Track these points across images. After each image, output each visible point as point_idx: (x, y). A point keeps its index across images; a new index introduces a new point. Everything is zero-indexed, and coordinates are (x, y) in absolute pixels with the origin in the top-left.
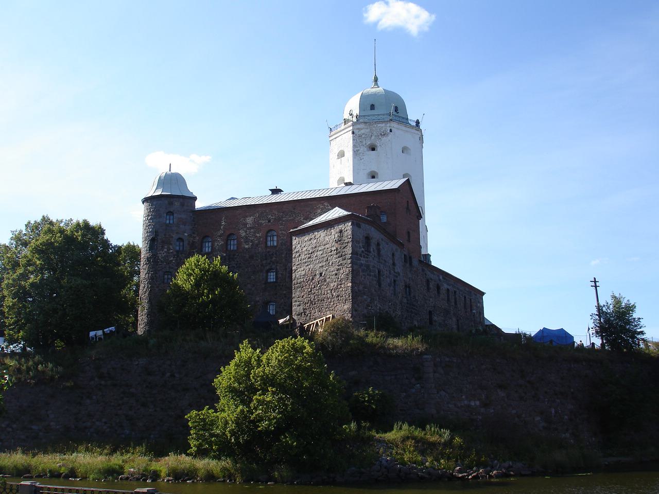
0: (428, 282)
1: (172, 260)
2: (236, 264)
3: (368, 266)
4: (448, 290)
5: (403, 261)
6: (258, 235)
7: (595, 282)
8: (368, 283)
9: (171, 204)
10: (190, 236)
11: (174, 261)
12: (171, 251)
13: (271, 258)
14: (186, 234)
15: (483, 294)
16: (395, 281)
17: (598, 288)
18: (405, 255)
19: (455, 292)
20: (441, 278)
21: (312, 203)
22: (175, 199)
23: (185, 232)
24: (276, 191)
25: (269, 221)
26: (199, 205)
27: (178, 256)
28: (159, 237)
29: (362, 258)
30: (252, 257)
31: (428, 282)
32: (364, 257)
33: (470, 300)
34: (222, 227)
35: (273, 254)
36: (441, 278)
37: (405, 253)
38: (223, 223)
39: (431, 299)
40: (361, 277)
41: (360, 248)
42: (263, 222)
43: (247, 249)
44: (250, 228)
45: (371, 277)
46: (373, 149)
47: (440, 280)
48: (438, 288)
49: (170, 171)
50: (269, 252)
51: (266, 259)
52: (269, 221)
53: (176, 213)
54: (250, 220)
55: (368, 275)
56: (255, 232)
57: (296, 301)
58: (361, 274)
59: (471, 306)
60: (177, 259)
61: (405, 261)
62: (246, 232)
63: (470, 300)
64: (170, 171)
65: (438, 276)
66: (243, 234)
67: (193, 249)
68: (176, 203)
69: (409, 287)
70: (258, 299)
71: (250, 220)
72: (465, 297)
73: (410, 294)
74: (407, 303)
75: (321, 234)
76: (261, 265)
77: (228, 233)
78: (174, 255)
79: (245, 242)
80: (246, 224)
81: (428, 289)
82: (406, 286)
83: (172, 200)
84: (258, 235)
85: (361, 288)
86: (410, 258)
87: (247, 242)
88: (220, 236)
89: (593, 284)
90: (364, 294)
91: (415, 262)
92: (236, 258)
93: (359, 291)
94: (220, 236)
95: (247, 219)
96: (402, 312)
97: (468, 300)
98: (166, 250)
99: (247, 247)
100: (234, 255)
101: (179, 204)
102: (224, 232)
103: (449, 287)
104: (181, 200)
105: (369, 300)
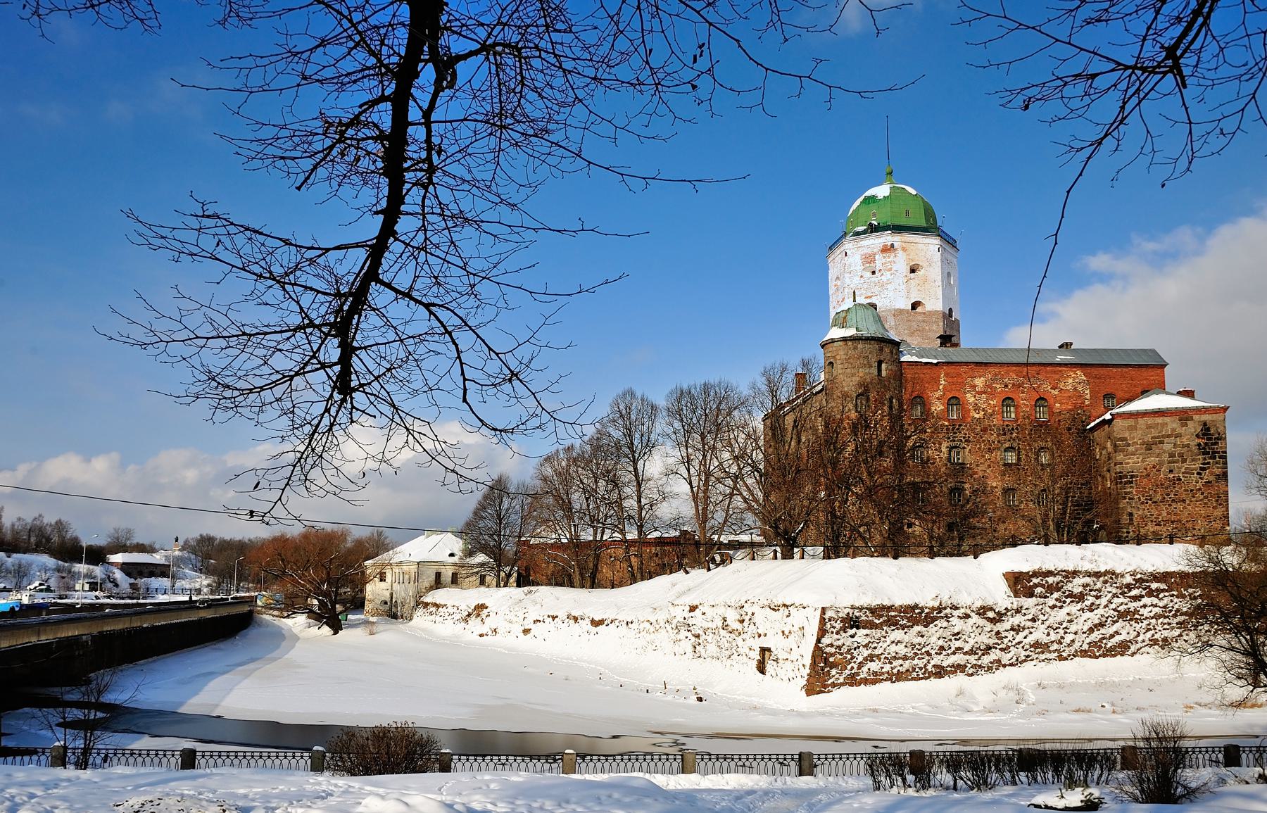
2: (964, 438)
6: (992, 402)
9: (881, 350)
13: (1012, 434)
21: (1060, 369)
25: (1006, 386)
34: (941, 387)
35: (1013, 429)
38: (943, 382)
42: (998, 386)
44: (982, 393)
50: (1007, 426)
51: (1005, 434)
52: (1006, 386)
54: (979, 382)
56: (987, 399)
57: (1125, 498)
62: (975, 396)
66: (972, 400)
76: (999, 442)
79: (975, 410)
80: (974, 387)
84: (992, 402)
87: (977, 409)
88: (938, 399)
92: (963, 429)
94: (938, 399)
99: (977, 416)
100: (960, 425)
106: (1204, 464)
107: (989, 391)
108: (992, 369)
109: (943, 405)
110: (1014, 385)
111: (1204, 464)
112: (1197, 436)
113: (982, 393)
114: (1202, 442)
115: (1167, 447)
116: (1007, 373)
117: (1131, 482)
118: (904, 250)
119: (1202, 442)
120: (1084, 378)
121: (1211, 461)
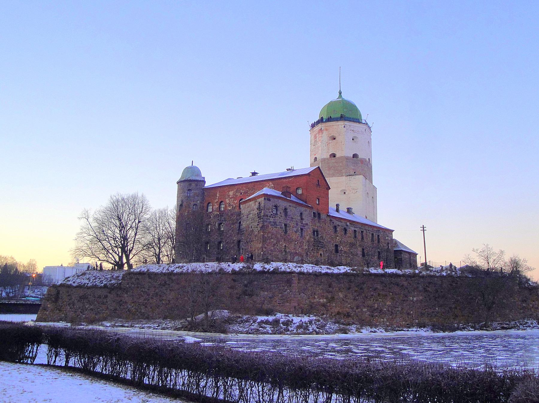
0: (335, 227)
2: (224, 219)
3: (275, 223)
4: (355, 231)
5: (312, 216)
6: (235, 202)
7: (423, 227)
8: (275, 232)
9: (190, 185)
10: (201, 203)
15: (393, 231)
16: (302, 229)
17: (425, 231)
18: (314, 213)
19: (362, 232)
20: (348, 224)
21: (263, 183)
24: (254, 174)
25: (241, 194)
26: (207, 185)
28: (184, 204)
29: (271, 218)
30: (232, 215)
31: (335, 227)
32: (273, 217)
33: (378, 236)
36: (348, 224)
37: (315, 212)
39: (337, 237)
40: (270, 229)
41: (270, 212)
42: (238, 194)
43: (230, 210)
44: (232, 198)
45: (278, 229)
46: (334, 139)
47: (347, 225)
48: (345, 230)
49: (192, 165)
52: (241, 194)
53: (193, 190)
54: (231, 193)
55: (275, 227)
56: (234, 200)
58: (270, 227)
59: (379, 239)
61: (315, 216)
63: (378, 236)
64: (192, 165)
65: (346, 223)
68: (193, 184)
69: (317, 231)
70: (234, 239)
71: (231, 193)
72: (372, 234)
73: (317, 235)
74: (314, 241)
75: (252, 203)
76: (237, 219)
81: (336, 231)
82: (314, 232)
84: (235, 202)
85: (270, 235)
86: (319, 214)
89: (422, 229)
90: (272, 238)
91: (323, 216)
93: (268, 237)
95: (230, 192)
96: (308, 247)
97: (376, 237)
99: (229, 209)
100: (223, 214)
102: (218, 200)
103: (356, 229)
105: (275, 241)
106: (258, 223)
107: (235, 197)
108: (236, 187)
109: (218, 205)
110: (244, 193)
111: (258, 223)
112: (257, 209)
113: (232, 198)
114: (258, 211)
115: (251, 215)
116: (242, 187)
117: (243, 234)
118: (326, 130)
119: (258, 211)
120: (273, 185)
121: (260, 221)
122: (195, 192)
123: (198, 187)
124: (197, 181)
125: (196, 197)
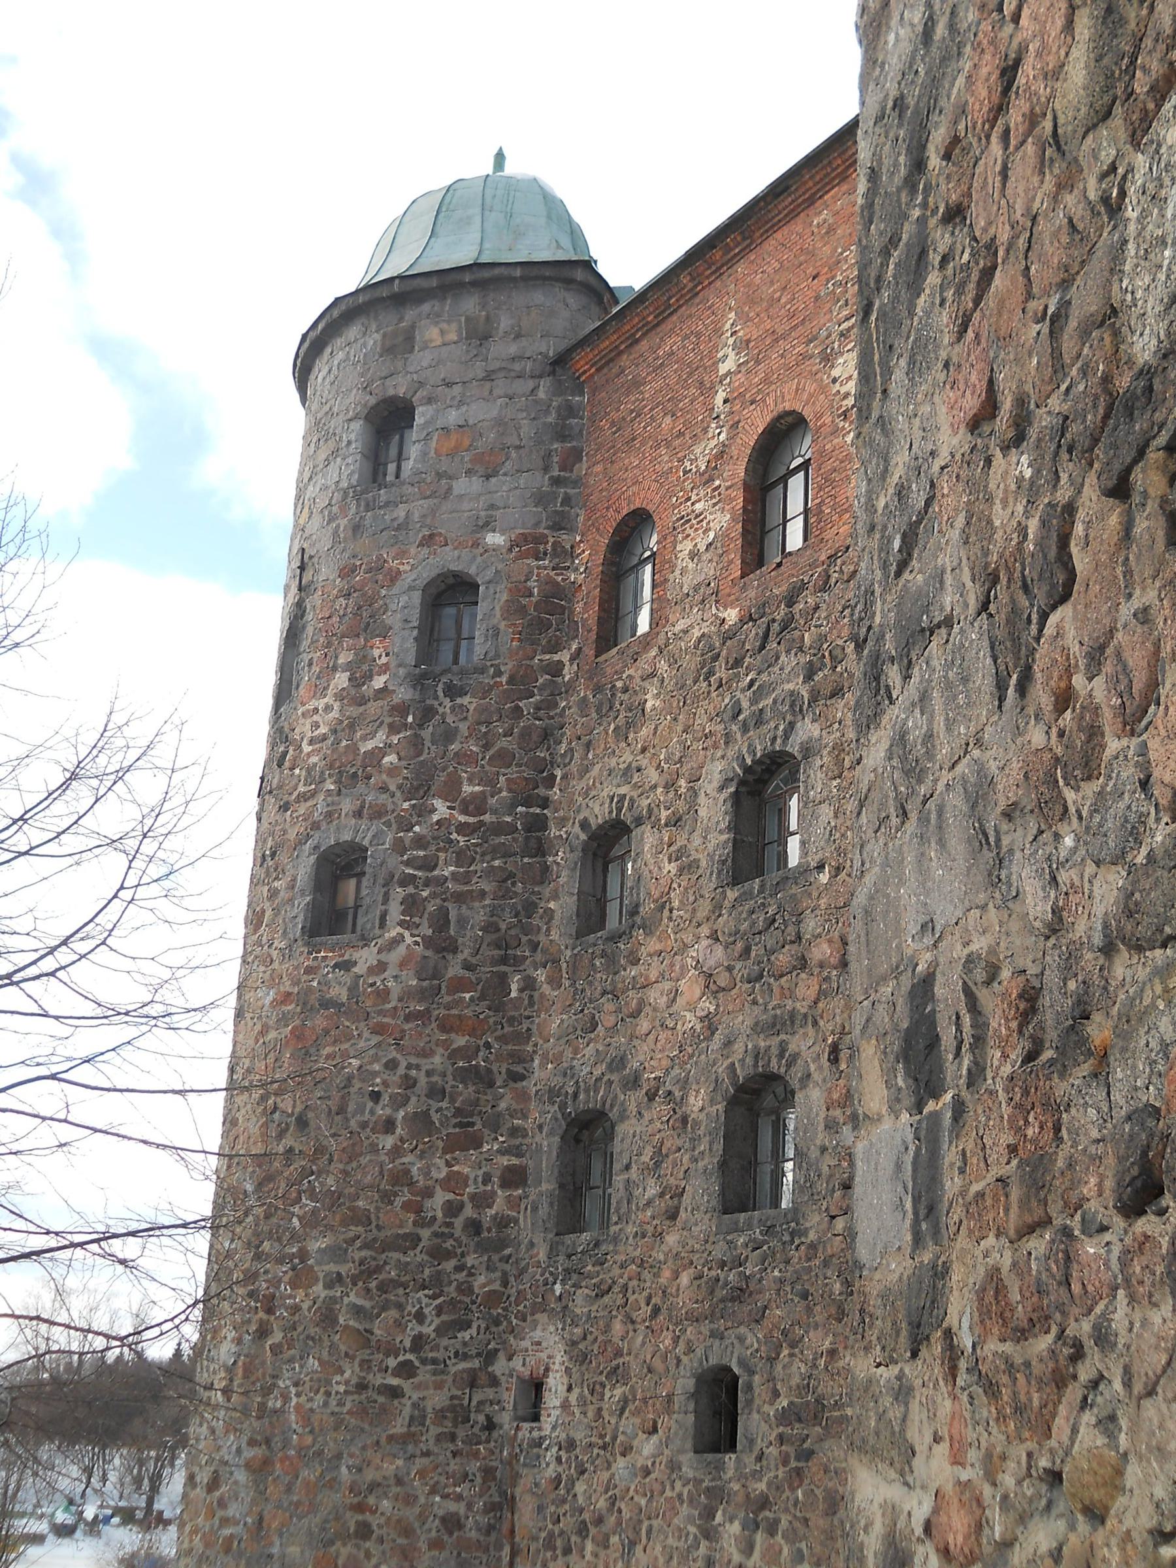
1: (376, 756)
11: (390, 759)
12: (379, 682)
14: (495, 539)
22: (426, 307)
23: (488, 525)
27: (427, 714)
53: (430, 400)
60: (416, 744)
67: (555, 648)
68: (432, 333)
77: (758, 422)
78: (401, 710)
83: (410, 314)
98: (341, 680)
101: (453, 336)
104: (470, 304)
122: (453, 417)
123: (501, 349)
124: (481, 285)
125: (461, 485)
